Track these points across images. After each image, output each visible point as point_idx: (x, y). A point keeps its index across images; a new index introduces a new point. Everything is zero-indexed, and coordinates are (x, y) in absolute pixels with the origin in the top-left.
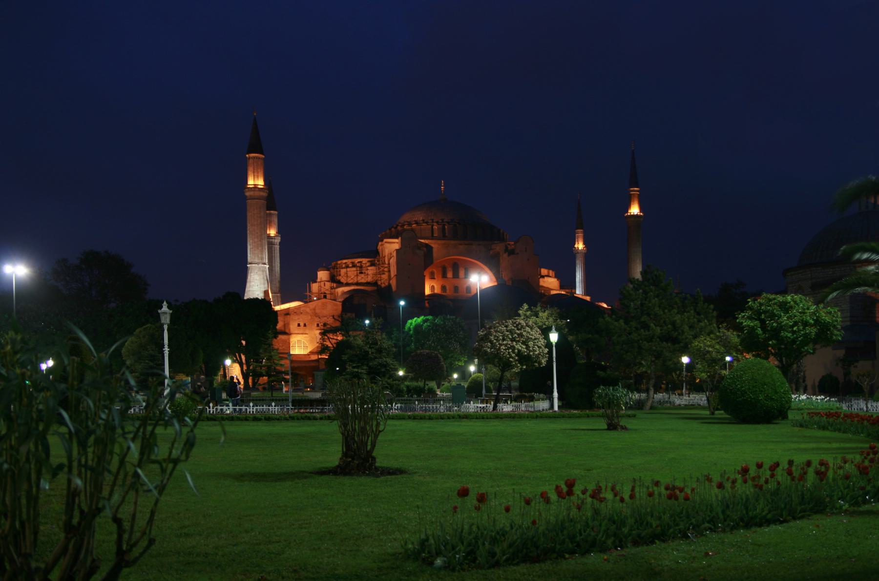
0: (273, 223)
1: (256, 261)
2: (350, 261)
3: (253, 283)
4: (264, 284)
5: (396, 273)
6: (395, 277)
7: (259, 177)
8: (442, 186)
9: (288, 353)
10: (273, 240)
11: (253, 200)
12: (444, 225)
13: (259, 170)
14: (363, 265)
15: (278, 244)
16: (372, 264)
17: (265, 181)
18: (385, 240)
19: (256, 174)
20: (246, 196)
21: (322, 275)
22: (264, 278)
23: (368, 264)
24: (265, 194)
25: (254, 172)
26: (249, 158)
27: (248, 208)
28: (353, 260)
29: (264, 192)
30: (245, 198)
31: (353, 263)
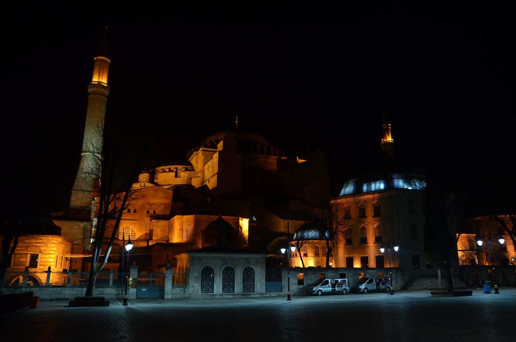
2: (167, 167)
6: (217, 175)
7: (104, 77)
8: (236, 121)
11: (94, 95)
13: (104, 71)
14: (177, 171)
16: (187, 170)
17: (108, 81)
19: (101, 74)
20: (88, 93)
21: (144, 177)
23: (184, 169)
24: (107, 93)
26: (97, 60)
27: (90, 102)
28: (169, 167)
30: (88, 94)
31: (169, 169)
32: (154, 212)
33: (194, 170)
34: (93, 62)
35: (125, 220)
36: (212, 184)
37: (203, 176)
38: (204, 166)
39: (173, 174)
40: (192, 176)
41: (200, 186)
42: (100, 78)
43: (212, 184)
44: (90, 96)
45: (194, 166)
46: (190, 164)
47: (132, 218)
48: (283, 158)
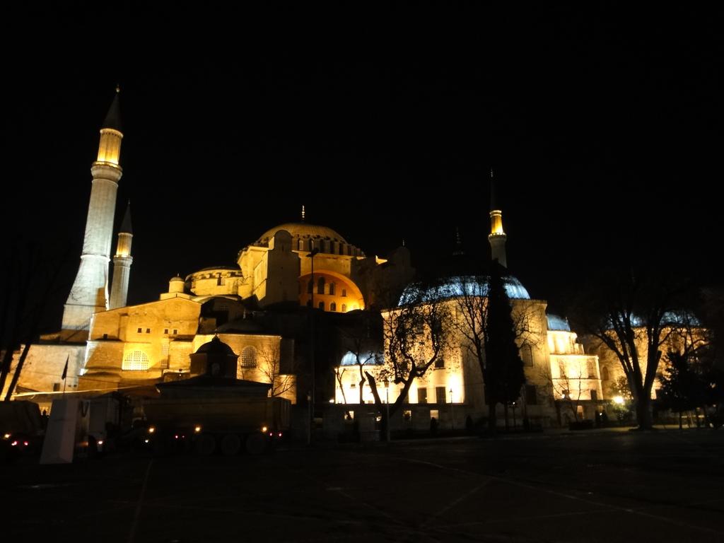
0: (126, 246)
1: (94, 251)
3: (84, 279)
4: (100, 280)
5: (266, 277)
9: (120, 369)
10: (124, 261)
12: (311, 240)
13: (114, 148)
15: (129, 266)
16: (233, 275)
18: (251, 248)
21: (176, 285)
22: (100, 272)
23: (230, 275)
24: (118, 176)
25: (107, 149)
26: (104, 134)
27: (93, 188)
28: (211, 272)
29: (116, 172)
30: (91, 178)
32: (175, 332)
33: (242, 276)
34: (99, 135)
35: (134, 342)
36: (260, 293)
37: (253, 283)
38: (254, 269)
39: (216, 281)
40: (240, 282)
41: (249, 295)
42: (108, 156)
43: (260, 293)
44: (94, 181)
45: (243, 270)
46: (238, 268)
47: (144, 340)
48: (359, 258)
